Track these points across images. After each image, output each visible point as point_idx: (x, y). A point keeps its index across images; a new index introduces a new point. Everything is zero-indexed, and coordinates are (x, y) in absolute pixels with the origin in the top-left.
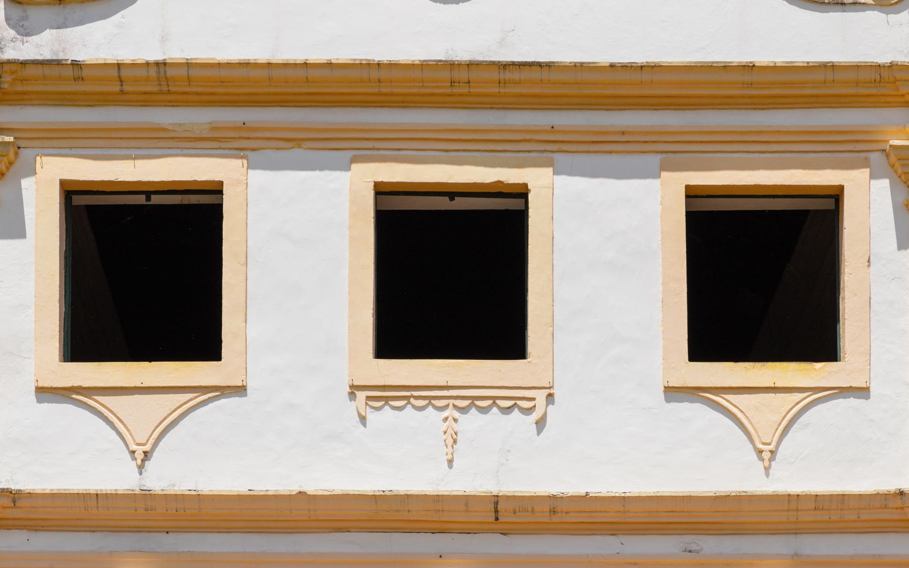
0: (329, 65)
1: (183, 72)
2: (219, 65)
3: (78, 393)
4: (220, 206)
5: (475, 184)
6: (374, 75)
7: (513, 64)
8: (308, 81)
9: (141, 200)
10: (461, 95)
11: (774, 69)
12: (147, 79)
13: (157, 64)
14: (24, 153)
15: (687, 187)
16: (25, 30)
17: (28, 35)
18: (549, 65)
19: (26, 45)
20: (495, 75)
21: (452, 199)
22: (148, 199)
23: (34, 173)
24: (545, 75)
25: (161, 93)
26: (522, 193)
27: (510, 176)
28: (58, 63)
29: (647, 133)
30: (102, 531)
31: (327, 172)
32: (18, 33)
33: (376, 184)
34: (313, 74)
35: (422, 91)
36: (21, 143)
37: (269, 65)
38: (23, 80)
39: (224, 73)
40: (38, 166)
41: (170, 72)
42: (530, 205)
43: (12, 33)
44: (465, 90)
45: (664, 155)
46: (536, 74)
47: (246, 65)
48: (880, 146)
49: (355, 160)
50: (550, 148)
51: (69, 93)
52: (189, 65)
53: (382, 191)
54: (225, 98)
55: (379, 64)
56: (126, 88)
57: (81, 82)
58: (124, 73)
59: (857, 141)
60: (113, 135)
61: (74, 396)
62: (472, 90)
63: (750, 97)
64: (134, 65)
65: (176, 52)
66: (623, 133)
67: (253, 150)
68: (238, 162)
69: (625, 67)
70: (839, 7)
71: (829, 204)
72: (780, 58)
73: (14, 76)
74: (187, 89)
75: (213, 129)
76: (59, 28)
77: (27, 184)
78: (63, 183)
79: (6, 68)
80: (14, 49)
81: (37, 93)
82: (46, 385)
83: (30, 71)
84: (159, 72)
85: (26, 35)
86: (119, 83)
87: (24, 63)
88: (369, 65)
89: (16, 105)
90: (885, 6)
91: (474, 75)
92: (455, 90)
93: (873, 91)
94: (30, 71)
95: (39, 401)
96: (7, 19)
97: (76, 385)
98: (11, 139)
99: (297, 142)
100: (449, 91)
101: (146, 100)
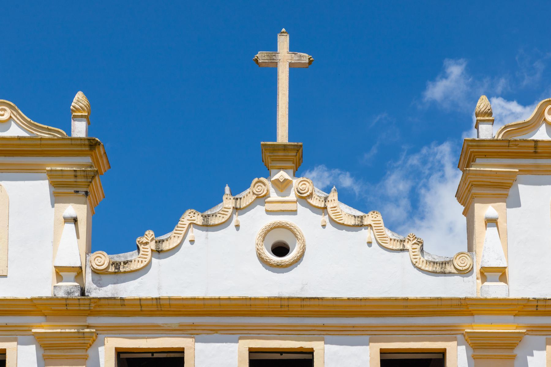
0: (229, 299)
1: (168, 302)
2: (183, 299)
4: (183, 358)
5: (291, 348)
6: (248, 303)
7: (307, 298)
8: (220, 306)
9: (149, 355)
10: (285, 311)
11: (416, 300)
12: (152, 305)
13: (156, 299)
15: (381, 349)
16: (100, 285)
17: (101, 287)
18: (322, 299)
20: (299, 303)
21: (281, 355)
22: (153, 355)
23: (104, 344)
24: (320, 303)
25: (158, 311)
26: (311, 352)
27: (306, 345)
28: (114, 299)
29: (364, 327)
31: (228, 344)
32: (97, 286)
33: (250, 349)
34: (222, 302)
35: (269, 309)
36: (98, 332)
37: (204, 299)
38: (99, 306)
39: (185, 302)
41: (162, 302)
42: (314, 357)
43: (95, 286)
44: (286, 309)
45: (371, 336)
46: (316, 302)
47: (194, 299)
48: (461, 332)
49: (240, 338)
50: (323, 333)
51: (119, 311)
52: (170, 299)
53: (252, 351)
54: (186, 313)
55: (250, 299)
56: (143, 309)
58: (142, 303)
62: (290, 309)
63: (407, 312)
64: (146, 299)
65: (165, 294)
66: (354, 327)
67: (197, 334)
68: (191, 340)
69: (354, 299)
71: (440, 356)
72: (419, 296)
74: (169, 309)
75: (180, 326)
76: (115, 284)
77: (101, 349)
78: (116, 349)
79: (92, 301)
81: (106, 311)
83: (102, 302)
84: (157, 302)
87: (100, 299)
88: (246, 299)
91: (290, 303)
92: (282, 309)
94: (102, 302)
96: (93, 280)
99: (216, 331)
100: (280, 309)
101: (151, 314)
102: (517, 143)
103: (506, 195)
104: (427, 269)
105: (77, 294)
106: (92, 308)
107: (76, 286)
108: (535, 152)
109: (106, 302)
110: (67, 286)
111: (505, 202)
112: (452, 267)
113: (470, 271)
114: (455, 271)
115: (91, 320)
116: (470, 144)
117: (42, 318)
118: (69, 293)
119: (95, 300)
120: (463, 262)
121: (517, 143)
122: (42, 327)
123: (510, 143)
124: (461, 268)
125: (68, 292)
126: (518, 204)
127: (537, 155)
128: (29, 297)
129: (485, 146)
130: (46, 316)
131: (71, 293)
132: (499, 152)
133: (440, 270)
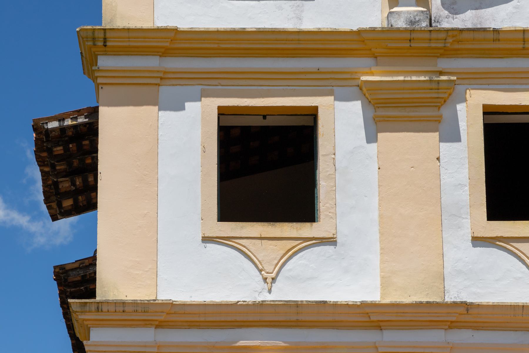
3: (500, 241)
14: (459, 88)
17: (457, 14)
19: (455, 20)
23: (465, 100)
30: (522, 330)
40: (468, 96)
43: (446, 12)
57: (497, 42)
60: (517, 76)
61: (498, 243)
73: (454, 39)
76: (477, 9)
77: (461, 108)
80: (447, 22)
82: (479, 236)
85: (455, 14)
86: (523, 43)
89: (451, 57)
95: (474, 246)
97: (499, 235)
98: (455, 78)
105: (424, 24)
106: (448, 45)
107: (422, 12)
109: (471, 35)
110: (409, 12)
115: (444, 64)
117: (368, 61)
118: (412, 23)
119: (455, 33)
122: (372, 74)
125: (411, 22)
128: (355, 29)
130: (376, 57)
131: (415, 22)
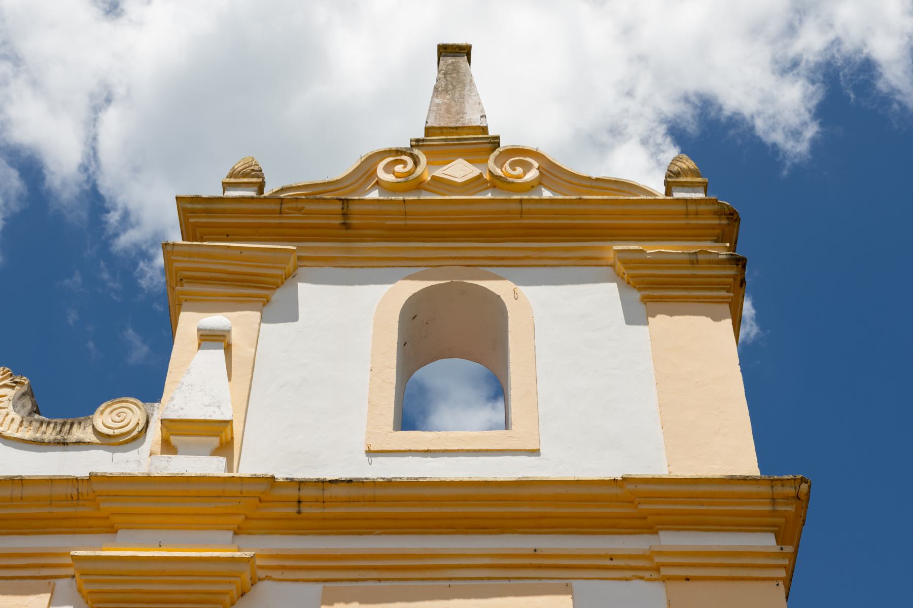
59: (43, 566)
70: (62, 447)
90: (114, 445)
93: (69, 511)
102: (300, 205)
103: (267, 302)
104: (18, 435)
108: (346, 226)
111: (261, 311)
112: (90, 430)
113: (134, 439)
114: (93, 438)
116: (189, 206)
120: (118, 419)
121: (300, 205)
123: (284, 206)
124: (110, 432)
126: (292, 316)
127: (350, 232)
129: (224, 212)
132: (260, 226)
133: (52, 438)
